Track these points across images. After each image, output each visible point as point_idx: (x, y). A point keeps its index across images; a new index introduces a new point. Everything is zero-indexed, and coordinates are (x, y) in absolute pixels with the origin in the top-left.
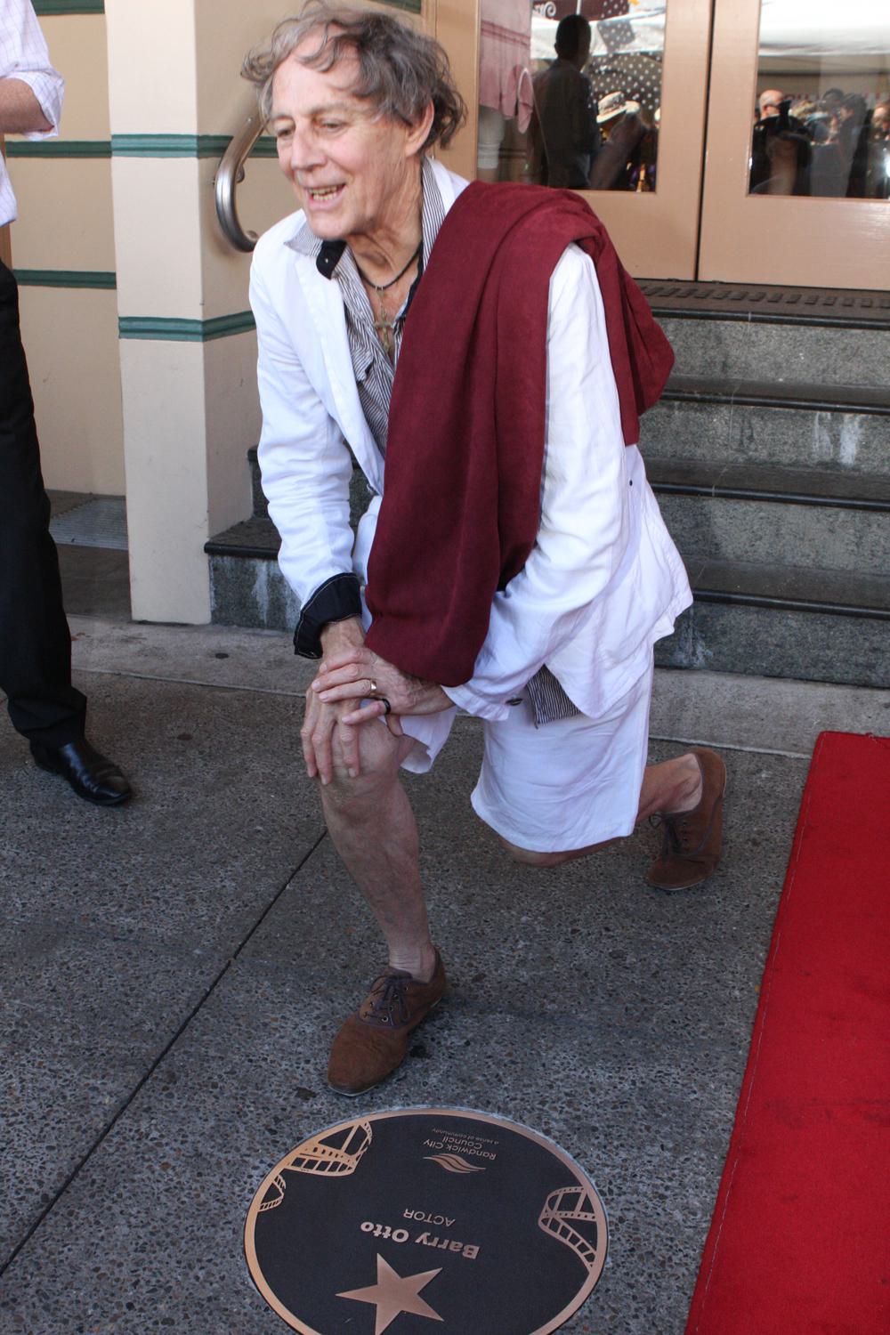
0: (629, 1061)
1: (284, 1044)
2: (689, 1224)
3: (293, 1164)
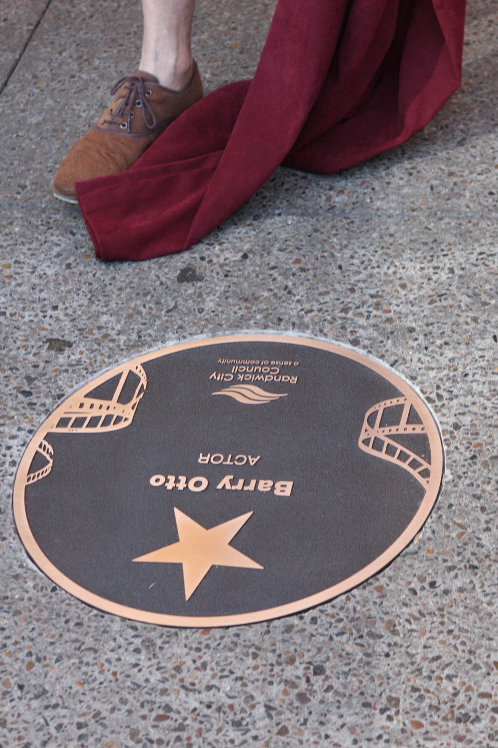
0: (443, 246)
1: (22, 293)
3: (57, 426)
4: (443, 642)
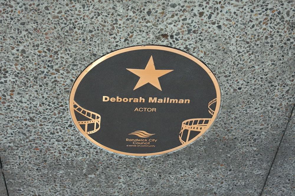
3: (208, 120)
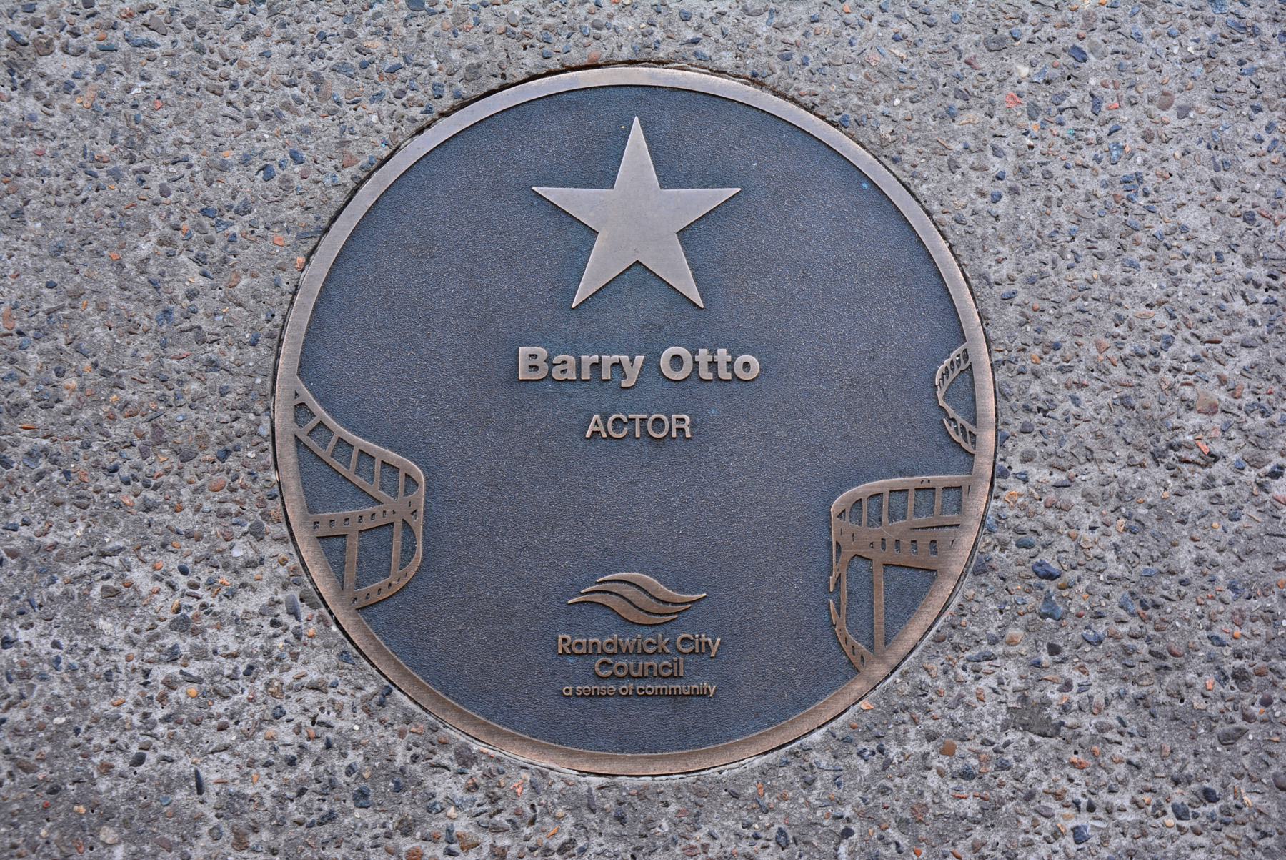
2: (115, 561)
4: (243, 66)
